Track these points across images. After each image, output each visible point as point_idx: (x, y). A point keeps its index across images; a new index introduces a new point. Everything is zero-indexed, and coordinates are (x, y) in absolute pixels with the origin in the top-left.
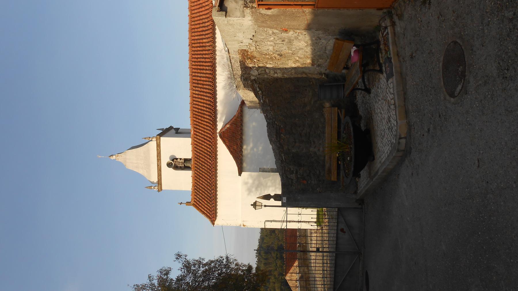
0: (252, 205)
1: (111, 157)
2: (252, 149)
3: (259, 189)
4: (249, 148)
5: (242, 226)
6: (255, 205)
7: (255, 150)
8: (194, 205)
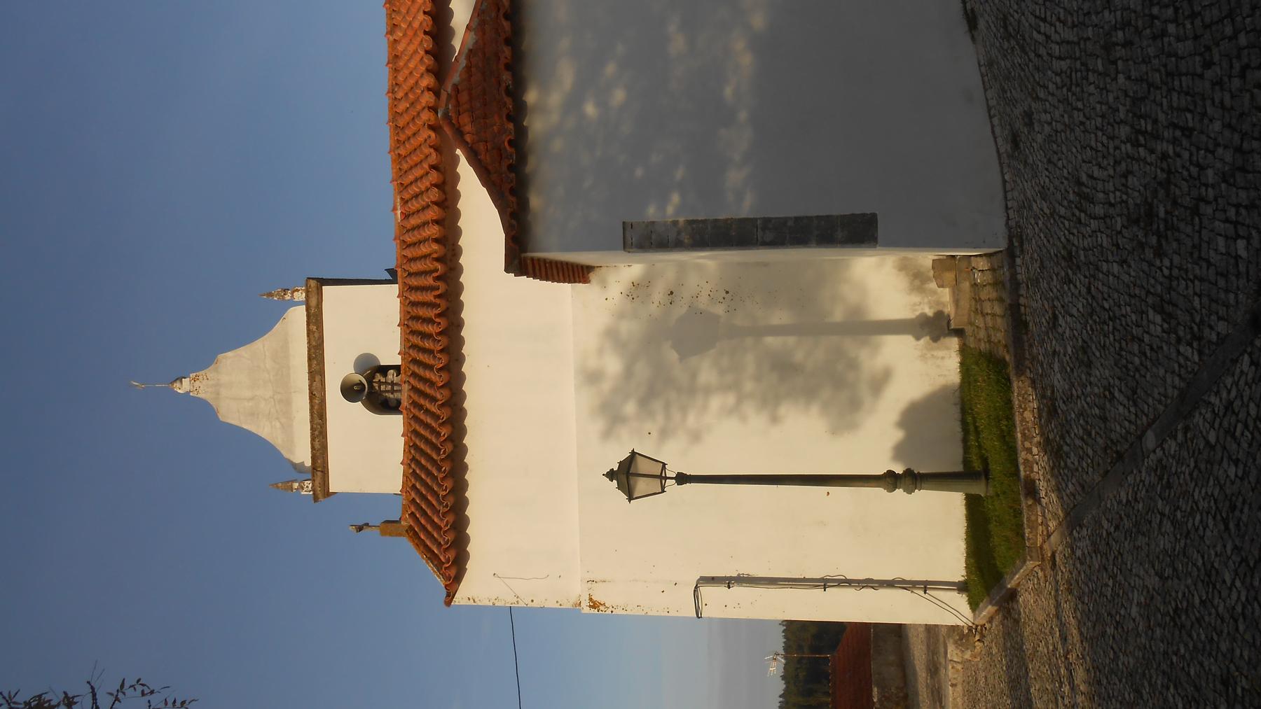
0: (611, 475)
1: (177, 385)
2: (573, 103)
3: (658, 405)
4: (555, 99)
5: (586, 610)
6: (626, 475)
7: (590, 109)
8: (412, 534)
